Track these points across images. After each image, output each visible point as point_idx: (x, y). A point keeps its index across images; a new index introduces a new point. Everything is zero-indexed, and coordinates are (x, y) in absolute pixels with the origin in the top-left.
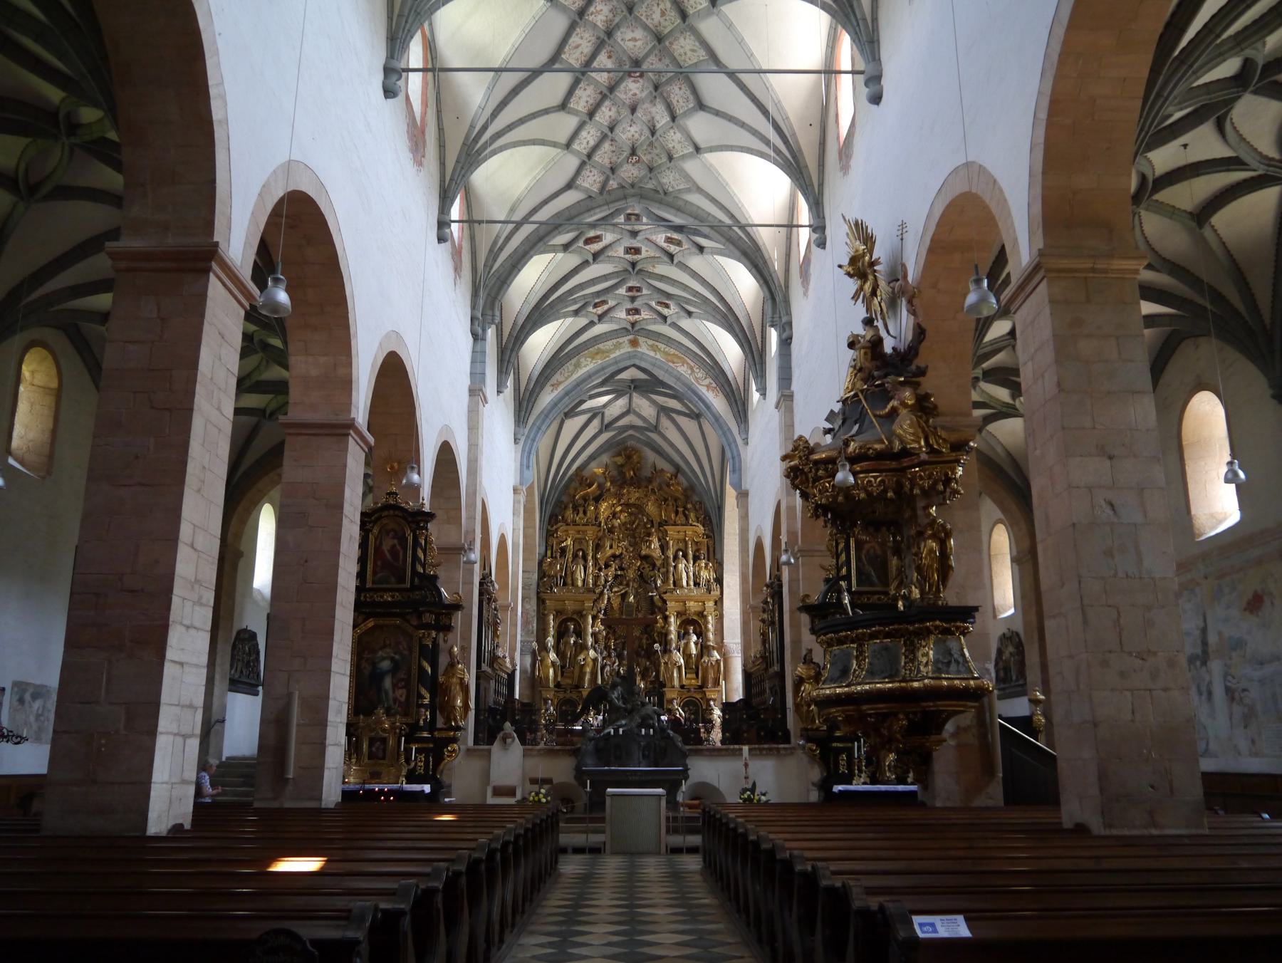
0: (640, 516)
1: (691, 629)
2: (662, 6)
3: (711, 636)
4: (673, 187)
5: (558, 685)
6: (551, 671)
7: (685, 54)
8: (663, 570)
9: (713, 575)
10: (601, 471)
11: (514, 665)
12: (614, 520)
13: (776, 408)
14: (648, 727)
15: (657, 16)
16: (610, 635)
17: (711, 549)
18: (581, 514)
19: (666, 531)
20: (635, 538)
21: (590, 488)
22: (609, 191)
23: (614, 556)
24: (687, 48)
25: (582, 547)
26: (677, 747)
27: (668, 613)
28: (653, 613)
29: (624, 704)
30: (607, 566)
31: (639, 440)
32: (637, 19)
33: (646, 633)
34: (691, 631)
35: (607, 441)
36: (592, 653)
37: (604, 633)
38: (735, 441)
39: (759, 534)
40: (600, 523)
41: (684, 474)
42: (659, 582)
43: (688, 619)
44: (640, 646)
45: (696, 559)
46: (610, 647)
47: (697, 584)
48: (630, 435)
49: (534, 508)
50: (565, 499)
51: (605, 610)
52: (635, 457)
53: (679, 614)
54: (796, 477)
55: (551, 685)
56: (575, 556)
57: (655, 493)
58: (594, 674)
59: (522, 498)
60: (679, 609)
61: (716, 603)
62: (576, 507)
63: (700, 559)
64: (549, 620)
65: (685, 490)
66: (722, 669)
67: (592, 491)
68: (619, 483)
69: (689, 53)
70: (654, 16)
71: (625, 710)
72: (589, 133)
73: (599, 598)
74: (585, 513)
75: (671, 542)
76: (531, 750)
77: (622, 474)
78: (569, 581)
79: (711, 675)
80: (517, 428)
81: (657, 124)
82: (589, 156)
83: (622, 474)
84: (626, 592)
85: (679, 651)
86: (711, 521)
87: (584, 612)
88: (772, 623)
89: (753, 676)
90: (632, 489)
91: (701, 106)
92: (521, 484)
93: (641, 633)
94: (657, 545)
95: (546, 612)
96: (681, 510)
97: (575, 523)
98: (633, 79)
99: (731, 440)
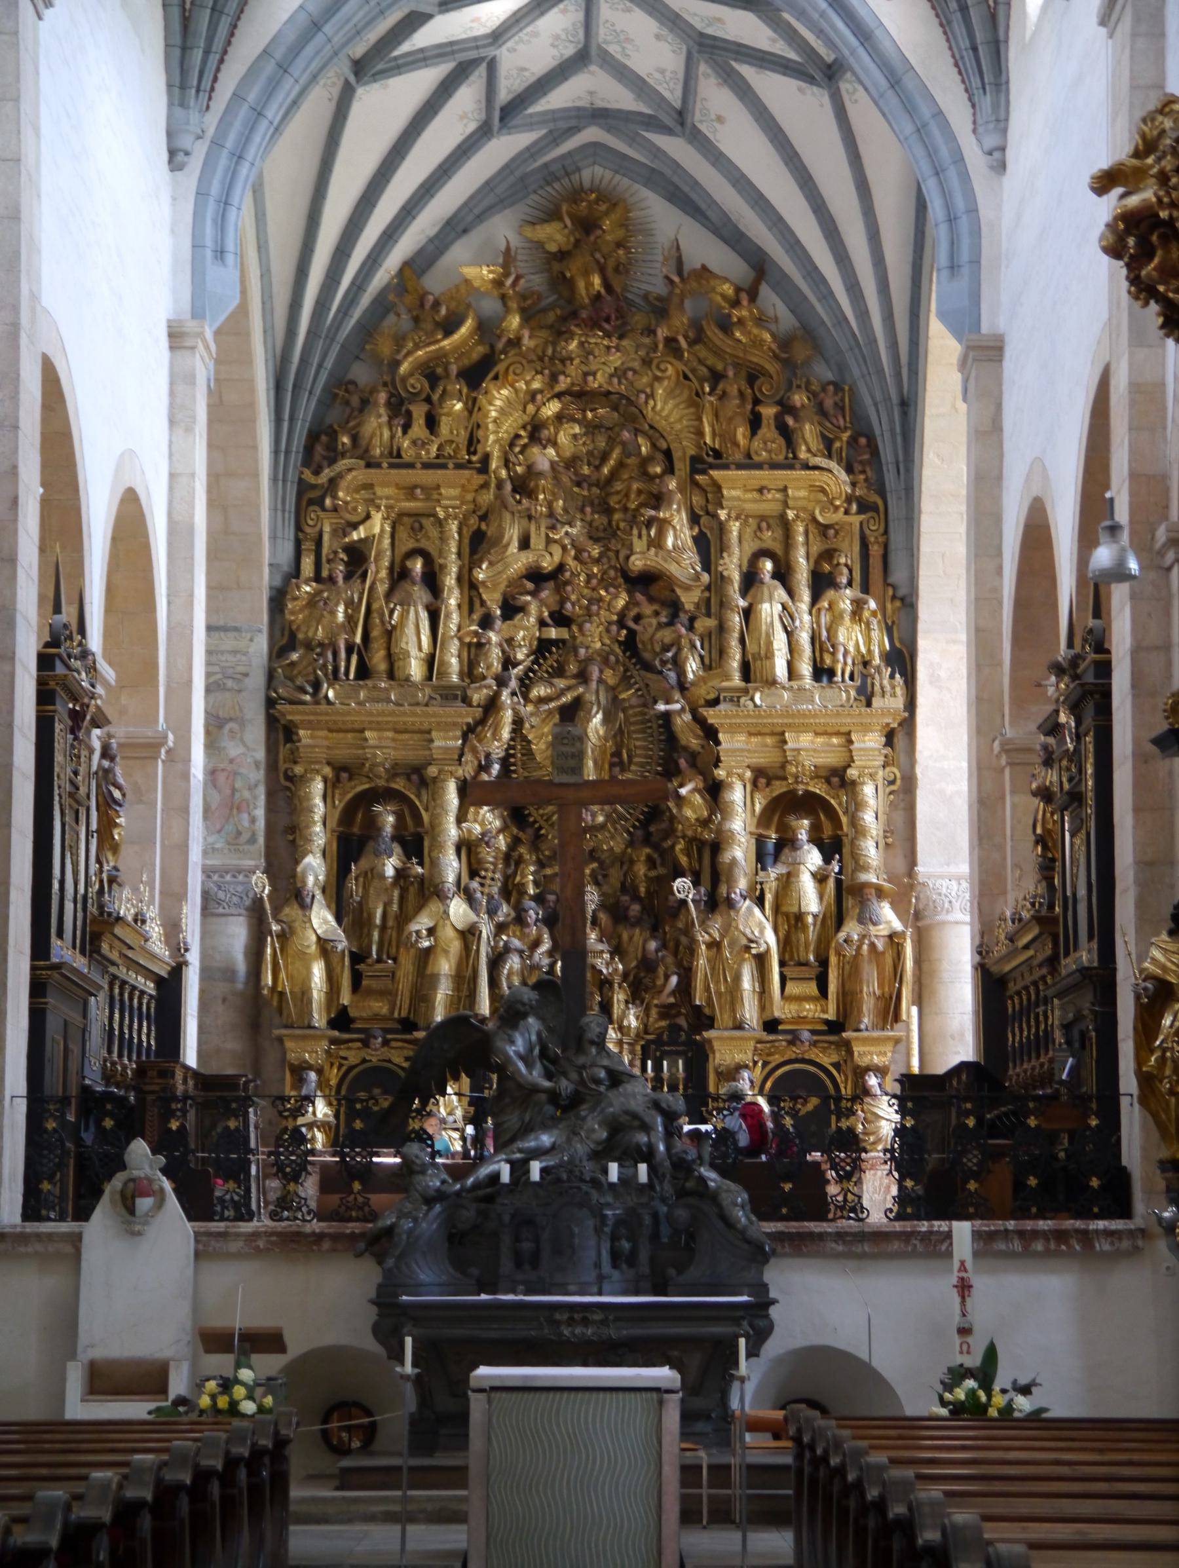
0: (626, 435)
1: (803, 828)
3: (871, 851)
5: (341, 1020)
6: (318, 971)
8: (705, 623)
9: (880, 642)
10: (486, 273)
11: (179, 950)
12: (535, 450)
13: (1103, 22)
14: (630, 1156)
16: (522, 850)
17: (875, 551)
18: (418, 429)
19: (718, 488)
20: (608, 511)
21: (448, 333)
23: (536, 576)
25: (424, 544)
26: (729, 1223)
28: (671, 771)
29: (549, 1076)
30: (511, 610)
31: (622, 163)
33: (647, 840)
34: (803, 836)
35: (507, 168)
36: (458, 910)
37: (502, 842)
38: (959, 159)
39: (1035, 491)
40: (486, 458)
41: (784, 286)
42: (692, 666)
43: (792, 793)
44: (629, 888)
45: (821, 583)
46: (522, 891)
47: (822, 673)
48: (595, 146)
49: (252, 405)
50: (361, 373)
51: (505, 762)
52: (607, 224)
53: (761, 777)
54: (1145, 253)
55: (319, 1019)
56: (399, 575)
57: (676, 352)
58: (465, 982)
59: (202, 367)
60: (760, 760)
61: (889, 737)
62: (401, 402)
63: (836, 586)
64: (308, 797)
65: (785, 343)
66: (909, 964)
67: (456, 348)
68: (551, 317)
71: (554, 1097)
73: (482, 722)
74: (432, 423)
75: (735, 527)
76: (223, 1235)
77: (562, 283)
78: (378, 660)
79: (871, 987)
80: (179, 112)
83: (562, 283)
84: (577, 703)
85: (760, 901)
86: (875, 452)
87: (432, 771)
88: (1075, 798)
89: (1012, 987)
90: (597, 339)
92: (197, 312)
93: (631, 844)
95: (298, 770)
96: (768, 412)
97: (396, 458)
99: (944, 153)
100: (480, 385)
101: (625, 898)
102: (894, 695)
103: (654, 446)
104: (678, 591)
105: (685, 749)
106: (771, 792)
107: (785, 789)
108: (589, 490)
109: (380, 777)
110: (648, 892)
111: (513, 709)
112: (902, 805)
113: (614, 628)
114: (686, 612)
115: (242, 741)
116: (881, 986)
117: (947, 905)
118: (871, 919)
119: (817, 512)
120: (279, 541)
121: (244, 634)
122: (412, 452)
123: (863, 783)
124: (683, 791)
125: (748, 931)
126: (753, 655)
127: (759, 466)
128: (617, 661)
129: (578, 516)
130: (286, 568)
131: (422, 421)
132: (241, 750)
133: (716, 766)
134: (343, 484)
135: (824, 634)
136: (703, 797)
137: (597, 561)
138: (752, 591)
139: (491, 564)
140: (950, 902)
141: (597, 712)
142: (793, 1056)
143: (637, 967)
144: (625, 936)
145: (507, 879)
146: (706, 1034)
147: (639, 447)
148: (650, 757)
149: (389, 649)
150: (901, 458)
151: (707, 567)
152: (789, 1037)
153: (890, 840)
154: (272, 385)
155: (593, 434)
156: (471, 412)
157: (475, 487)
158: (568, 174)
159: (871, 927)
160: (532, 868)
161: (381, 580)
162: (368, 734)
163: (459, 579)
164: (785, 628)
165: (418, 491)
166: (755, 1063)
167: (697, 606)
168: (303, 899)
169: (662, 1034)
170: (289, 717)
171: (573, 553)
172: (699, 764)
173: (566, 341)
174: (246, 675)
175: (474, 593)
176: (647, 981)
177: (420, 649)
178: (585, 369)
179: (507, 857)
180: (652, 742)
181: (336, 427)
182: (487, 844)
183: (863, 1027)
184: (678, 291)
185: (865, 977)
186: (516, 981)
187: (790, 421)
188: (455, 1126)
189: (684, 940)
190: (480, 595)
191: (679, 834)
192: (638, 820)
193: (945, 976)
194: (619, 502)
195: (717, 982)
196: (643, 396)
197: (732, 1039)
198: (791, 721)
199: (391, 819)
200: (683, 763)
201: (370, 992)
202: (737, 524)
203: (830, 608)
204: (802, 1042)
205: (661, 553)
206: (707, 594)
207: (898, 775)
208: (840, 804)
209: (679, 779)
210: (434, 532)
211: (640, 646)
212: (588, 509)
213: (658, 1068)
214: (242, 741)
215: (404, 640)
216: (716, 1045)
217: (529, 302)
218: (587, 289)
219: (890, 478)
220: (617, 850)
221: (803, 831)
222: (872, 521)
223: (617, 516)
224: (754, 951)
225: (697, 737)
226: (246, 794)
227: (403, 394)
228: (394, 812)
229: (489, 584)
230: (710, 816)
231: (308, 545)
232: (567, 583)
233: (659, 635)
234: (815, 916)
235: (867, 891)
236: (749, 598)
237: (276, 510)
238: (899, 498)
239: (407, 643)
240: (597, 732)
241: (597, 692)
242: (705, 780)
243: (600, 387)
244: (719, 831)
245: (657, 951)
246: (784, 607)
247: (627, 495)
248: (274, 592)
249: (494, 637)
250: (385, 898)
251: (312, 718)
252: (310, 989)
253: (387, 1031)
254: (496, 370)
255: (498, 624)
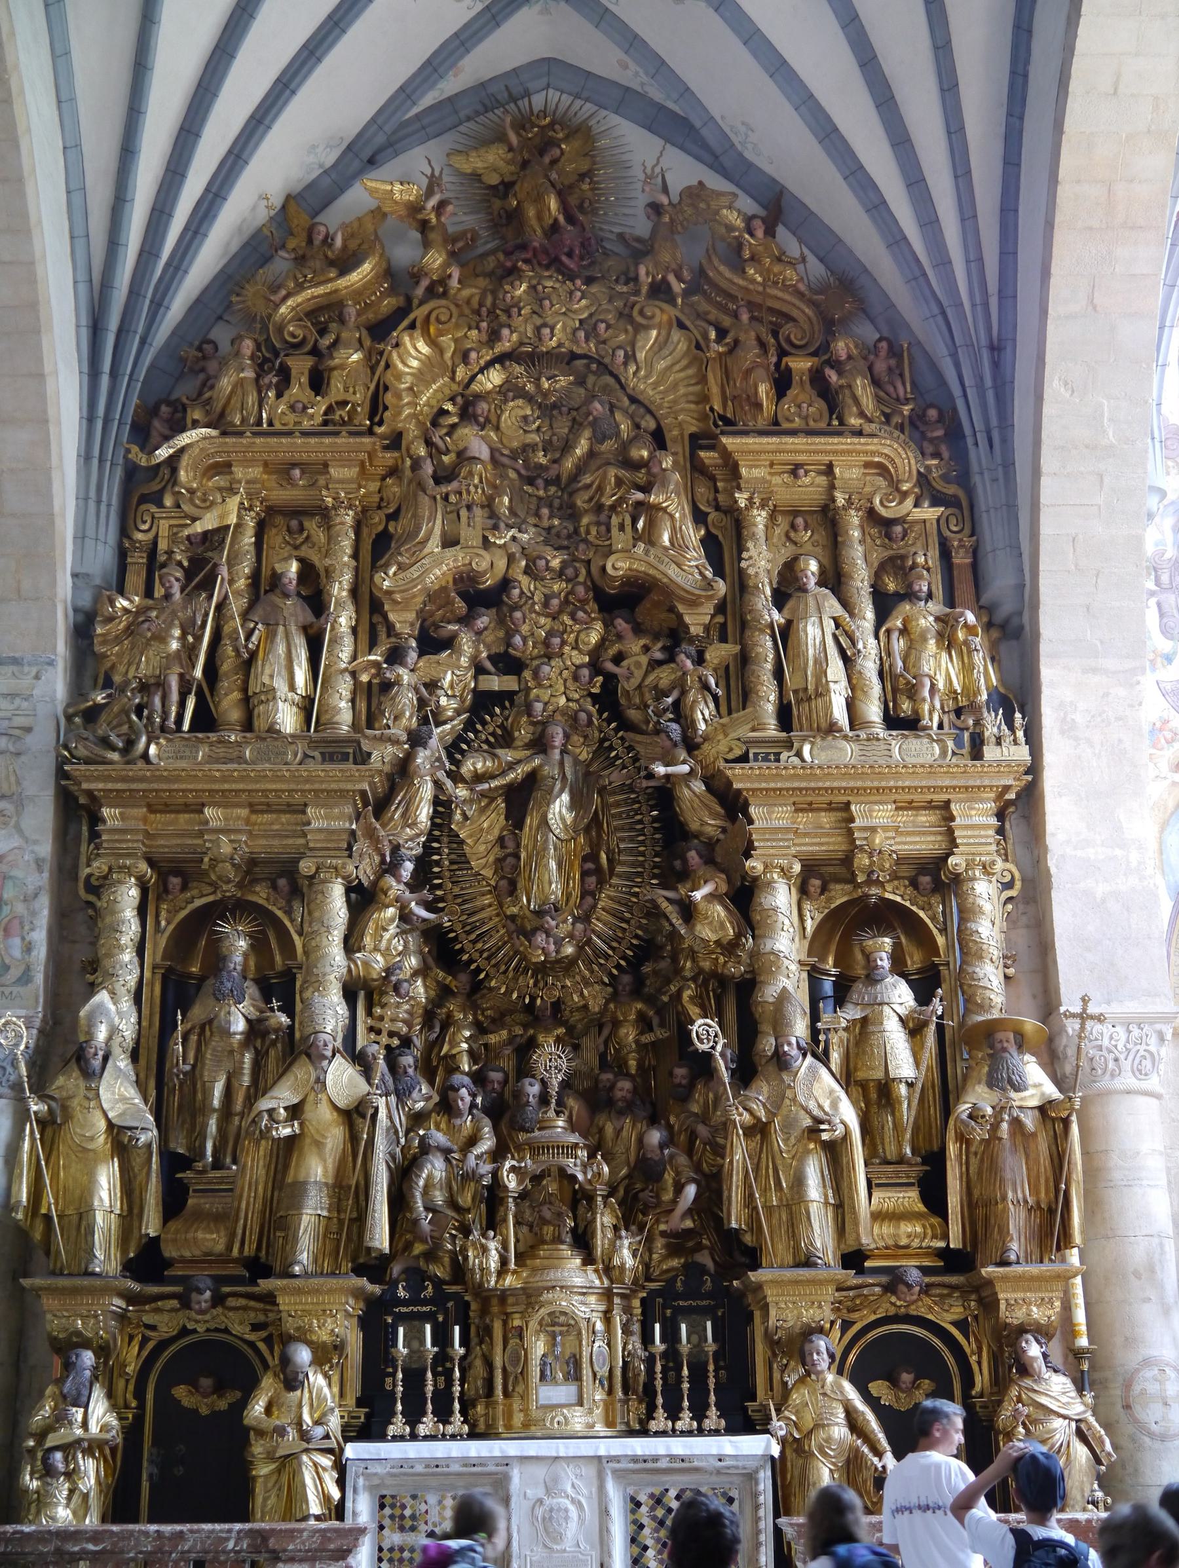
1: (883, 947)
17: (961, 559)
18: (298, 390)
21: (344, 271)
27: (754, 865)
33: (637, 992)
34: (885, 962)
37: (419, 989)
42: (703, 714)
44: (611, 1062)
51: (423, 864)
64: (113, 909)
67: (358, 294)
74: (318, 383)
75: (760, 518)
78: (229, 705)
84: (532, 778)
85: (823, 1058)
87: (306, 866)
93: (614, 997)
94: (693, 535)
100: (389, 333)
101: (607, 1077)
102: (1015, 742)
103: (637, 426)
104: (681, 608)
105: (696, 836)
106: (829, 900)
107: (844, 899)
108: (546, 490)
109: (229, 881)
110: (640, 1066)
111: (437, 784)
112: (1024, 919)
113: (585, 672)
114: (691, 640)
115: (18, 827)
116: (1034, 1189)
117: (1111, 1065)
118: (1010, 1081)
119: (877, 501)
120: (89, 543)
121: (26, 669)
122: (291, 418)
123: (974, 879)
124: (698, 895)
125: (812, 1105)
126: (796, 692)
127: (793, 433)
128: (590, 723)
129: (532, 520)
130: (98, 581)
131: (304, 379)
132: (16, 842)
133: (748, 855)
134: (185, 461)
135: (900, 664)
136: (726, 908)
137: (560, 574)
138: (790, 604)
139: (401, 568)
140: (1116, 1060)
141: (562, 791)
142: (892, 1311)
143: (629, 1176)
144: (609, 1129)
145: (432, 1046)
146: (753, 1276)
147: (618, 426)
148: (642, 864)
149: (245, 690)
150: (994, 422)
151: (719, 572)
152: (884, 1279)
153: (1011, 971)
154: (84, 321)
155: (551, 417)
156: (373, 369)
157: (381, 471)
158: (514, 99)
159: (1013, 1095)
160: (467, 1034)
161: (237, 593)
162: (208, 812)
163: (354, 592)
164: (842, 652)
165: (297, 473)
166: (832, 1323)
167: (707, 628)
168: (87, 1061)
169: (673, 1280)
170: (85, 786)
171: (524, 563)
172: (719, 860)
173: (512, 284)
174: (29, 730)
175: (377, 618)
176: (646, 1195)
177: (292, 688)
178: (539, 322)
179: (429, 1017)
180: (642, 843)
181: (185, 400)
182: (396, 988)
183: (1013, 1257)
184: (666, 219)
185: (1008, 1175)
186: (439, 1198)
187: (833, 376)
188: (326, 1444)
189: (702, 1130)
190: (385, 617)
191: (688, 974)
192: (624, 958)
193: (1117, 1175)
194: (591, 499)
195: (765, 1191)
196: (621, 353)
197: (796, 1282)
198: (859, 784)
199: (243, 944)
200: (693, 856)
201: (200, 1216)
202: (764, 514)
203: (904, 631)
204: (909, 1287)
205: (652, 551)
206: (720, 619)
207: (1017, 875)
208: (933, 919)
209: (688, 886)
210: (320, 536)
211: (623, 701)
212: (545, 511)
213: (670, 1336)
214: (18, 827)
215: (267, 671)
216: (770, 1293)
217: (460, 244)
218: (539, 218)
219: (978, 456)
220: (595, 1006)
221: (884, 955)
222: (953, 520)
223: (585, 521)
224: (825, 1136)
225: (714, 815)
226: (20, 908)
227: (278, 345)
228: (250, 935)
229: (398, 597)
230: (739, 935)
231: (138, 559)
232: (516, 607)
233: (651, 678)
234: (910, 1085)
235: (1000, 1035)
236: (786, 610)
237: (86, 499)
238: (995, 480)
239: (272, 676)
240: (563, 819)
241: (562, 763)
242: (729, 881)
243: (560, 345)
244: (755, 954)
245: (662, 1146)
246: (837, 626)
247: (600, 489)
248: (81, 618)
249: (406, 676)
250: (228, 1065)
251: (119, 786)
252: (91, 1210)
253: (219, 1280)
254: (412, 316)
255: (413, 656)
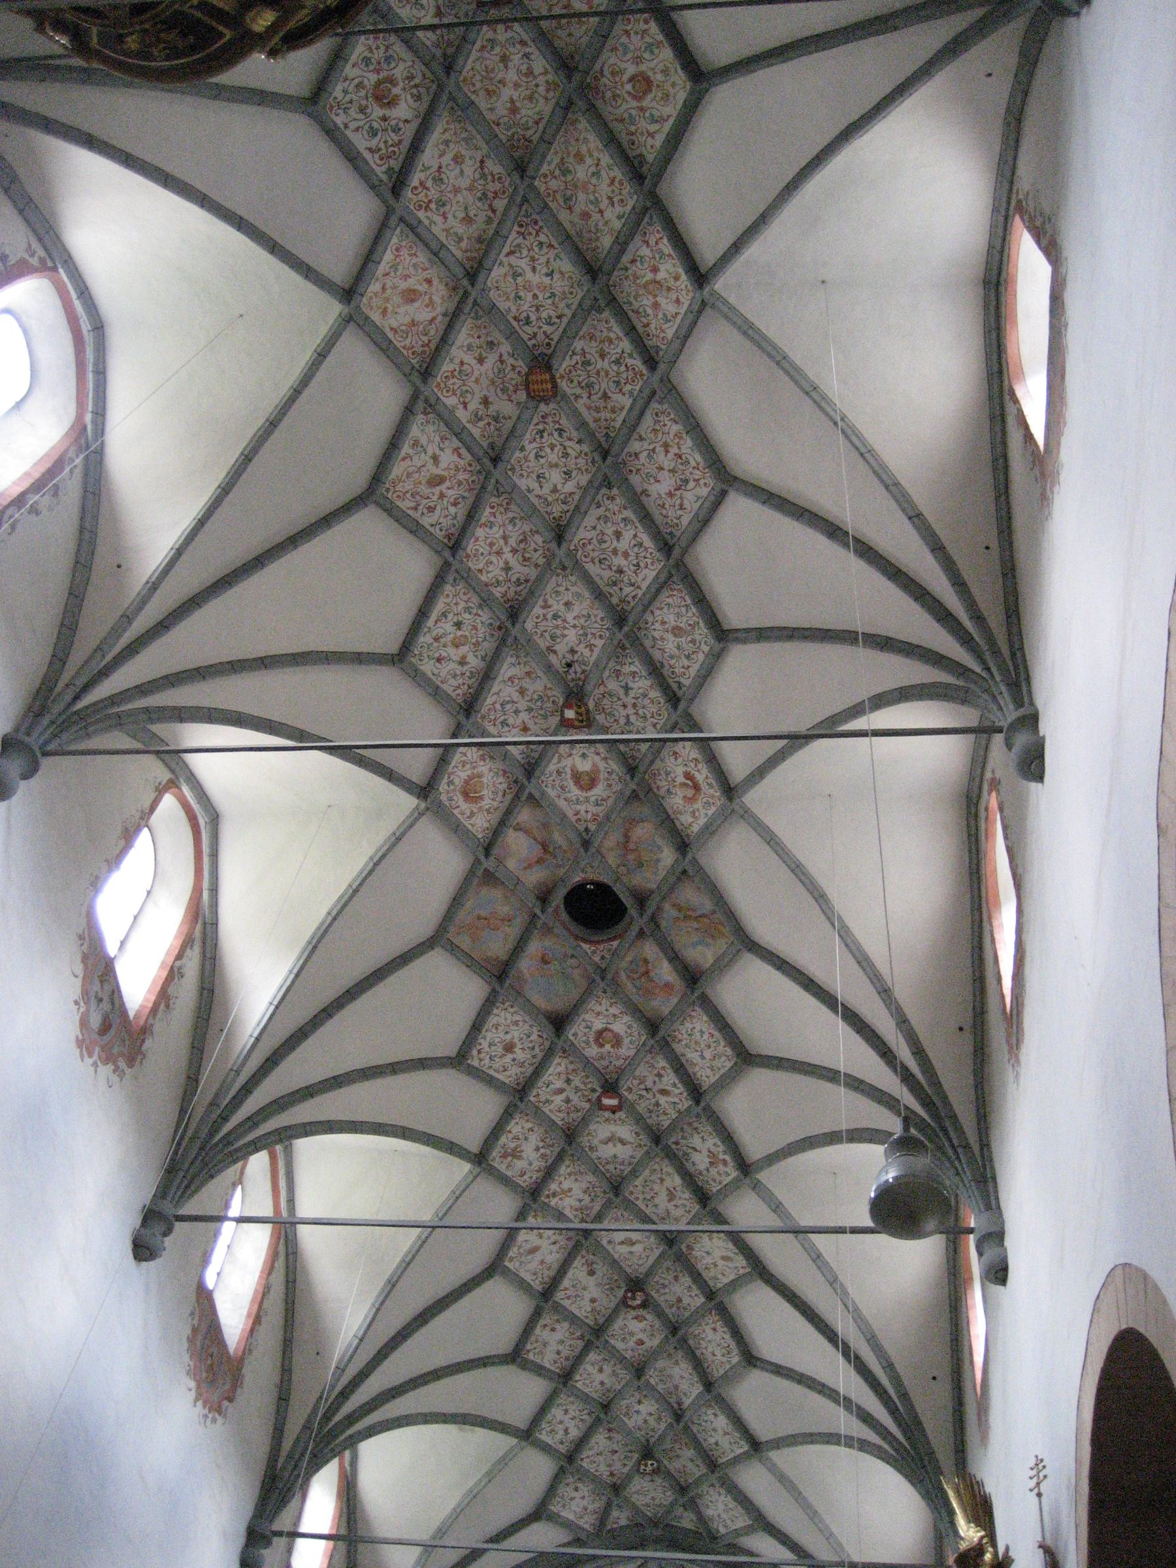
2: (668, 1183)
4: (726, 1526)
7: (716, 1266)
15: (662, 1200)
22: (613, 1530)
24: (717, 1254)
32: (629, 1205)
69: (720, 1263)
70: (657, 1201)
72: (566, 1412)
81: (684, 1399)
82: (570, 1458)
91: (751, 1359)
98: (633, 1313)
